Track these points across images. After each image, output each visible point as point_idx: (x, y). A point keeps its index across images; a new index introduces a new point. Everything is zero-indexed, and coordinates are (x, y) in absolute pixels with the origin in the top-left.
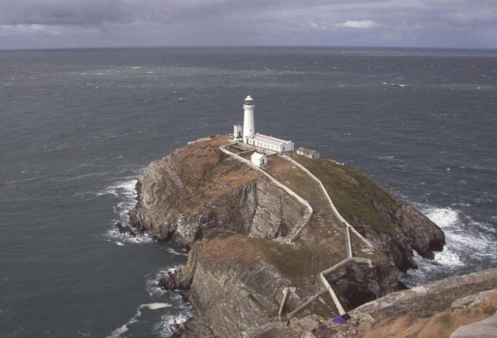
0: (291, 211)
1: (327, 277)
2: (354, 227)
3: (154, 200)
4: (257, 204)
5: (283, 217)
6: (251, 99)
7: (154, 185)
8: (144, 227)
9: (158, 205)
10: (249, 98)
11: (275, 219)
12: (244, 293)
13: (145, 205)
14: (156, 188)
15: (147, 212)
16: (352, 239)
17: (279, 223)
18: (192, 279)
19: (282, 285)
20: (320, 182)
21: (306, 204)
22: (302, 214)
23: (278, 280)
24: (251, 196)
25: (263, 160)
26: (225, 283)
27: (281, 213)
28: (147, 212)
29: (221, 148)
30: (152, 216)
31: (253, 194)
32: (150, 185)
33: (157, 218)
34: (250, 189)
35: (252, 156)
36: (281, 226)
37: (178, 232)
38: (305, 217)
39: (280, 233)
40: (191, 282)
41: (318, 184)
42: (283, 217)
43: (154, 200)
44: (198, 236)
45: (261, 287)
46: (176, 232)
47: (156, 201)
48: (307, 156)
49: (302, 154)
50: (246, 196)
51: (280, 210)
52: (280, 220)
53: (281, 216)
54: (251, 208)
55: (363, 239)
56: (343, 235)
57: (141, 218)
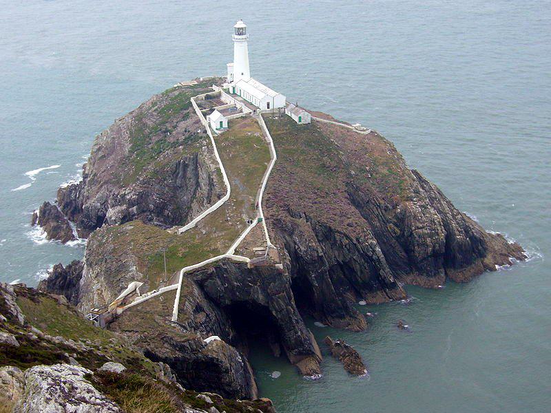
8: (75, 208)
10: (240, 25)
19: (133, 279)
25: (221, 122)
51: (208, 194)
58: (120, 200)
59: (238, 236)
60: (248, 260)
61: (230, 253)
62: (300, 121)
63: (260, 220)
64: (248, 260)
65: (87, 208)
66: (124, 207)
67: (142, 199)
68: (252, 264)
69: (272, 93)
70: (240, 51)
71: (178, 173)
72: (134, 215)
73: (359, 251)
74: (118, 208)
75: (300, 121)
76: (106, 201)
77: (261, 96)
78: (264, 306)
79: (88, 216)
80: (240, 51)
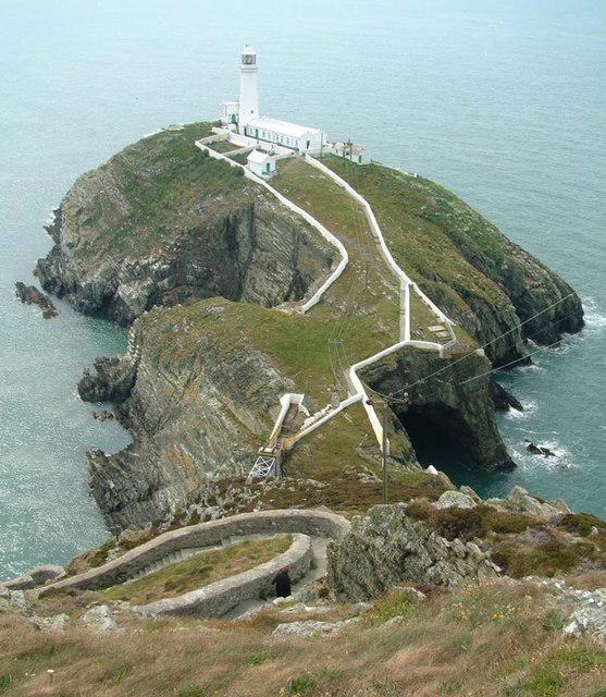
0: (310, 256)
1: (362, 374)
2: (419, 286)
3: (79, 241)
4: (254, 245)
5: (298, 267)
7: (79, 212)
8: (62, 287)
9: (84, 249)
11: (284, 273)
12: (214, 403)
13: (65, 249)
14: (84, 218)
17: (291, 279)
18: (135, 378)
19: (282, 390)
20: (366, 203)
21: (340, 245)
22: (330, 260)
23: (274, 381)
24: (243, 230)
26: (186, 386)
27: (294, 261)
29: (197, 143)
32: (73, 212)
33: (84, 273)
35: (249, 158)
36: (294, 283)
37: (119, 297)
38: (333, 267)
39: (293, 296)
40: (133, 384)
41: (361, 208)
42: (298, 267)
43: (79, 241)
44: (153, 298)
45: (244, 394)
46: (116, 296)
47: (83, 240)
48: (348, 157)
49: (340, 154)
55: (435, 309)
56: (397, 299)
57: (58, 272)
58: (135, 275)
59: (398, 313)
60: (440, 347)
61: (406, 340)
62: (360, 161)
63: (411, 287)
64: (440, 347)
66: (149, 281)
67: (177, 267)
68: (445, 352)
73: (497, 321)
75: (360, 161)
76: (115, 275)
78: (451, 410)
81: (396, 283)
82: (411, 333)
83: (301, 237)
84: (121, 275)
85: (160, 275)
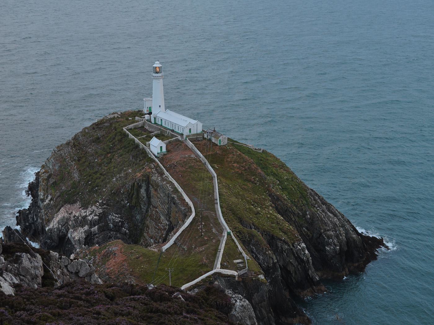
6: (160, 65)
7: (49, 177)
8: (35, 230)
10: (157, 64)
14: (52, 181)
15: (40, 211)
16: (232, 244)
20: (216, 175)
25: (161, 147)
28: (40, 211)
30: (44, 217)
31: (145, 190)
34: (142, 183)
42: (171, 219)
44: (89, 240)
50: (138, 192)
51: (168, 212)
52: (168, 223)
53: (169, 218)
54: (144, 208)
57: (33, 219)
59: (216, 250)
60: (235, 273)
61: (218, 269)
63: (229, 234)
64: (235, 273)
65: (50, 230)
66: (86, 228)
68: (239, 276)
69: (194, 122)
70: (158, 87)
71: (133, 195)
72: (96, 234)
74: (81, 230)
77: (184, 124)
79: (50, 238)
80: (158, 87)
81: (221, 230)
82: (221, 264)
83: (173, 201)
84: (70, 223)
85: (92, 224)
